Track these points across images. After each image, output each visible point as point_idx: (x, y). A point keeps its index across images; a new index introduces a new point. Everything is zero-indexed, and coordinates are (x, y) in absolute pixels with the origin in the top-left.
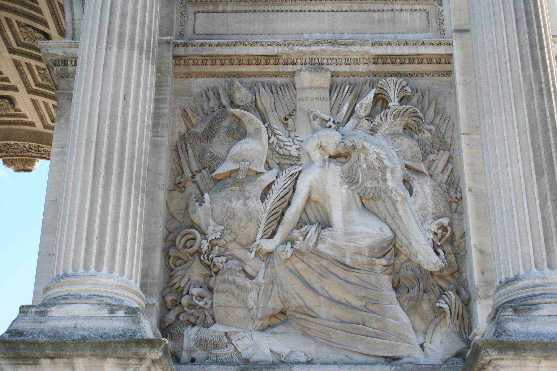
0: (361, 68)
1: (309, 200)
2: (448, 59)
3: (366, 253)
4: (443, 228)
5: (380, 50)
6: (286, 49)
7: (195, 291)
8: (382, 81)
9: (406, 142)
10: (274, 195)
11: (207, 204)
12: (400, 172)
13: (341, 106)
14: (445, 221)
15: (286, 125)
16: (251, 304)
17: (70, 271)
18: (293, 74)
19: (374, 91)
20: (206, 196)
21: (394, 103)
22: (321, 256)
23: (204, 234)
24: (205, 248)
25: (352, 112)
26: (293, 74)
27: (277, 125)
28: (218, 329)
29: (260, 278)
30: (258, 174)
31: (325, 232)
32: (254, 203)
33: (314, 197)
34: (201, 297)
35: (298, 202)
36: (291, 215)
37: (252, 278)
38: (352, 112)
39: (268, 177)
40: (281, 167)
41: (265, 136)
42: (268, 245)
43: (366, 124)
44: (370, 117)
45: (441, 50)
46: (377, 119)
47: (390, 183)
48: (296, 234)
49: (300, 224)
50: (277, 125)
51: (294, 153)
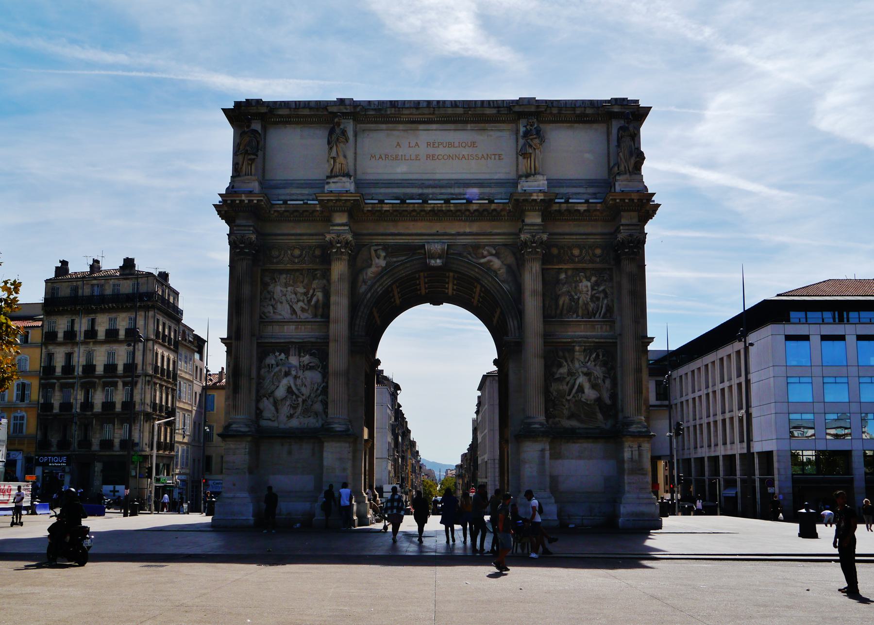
0: (592, 344)
1: (579, 386)
2: (616, 342)
3: (593, 401)
4: (612, 393)
5: (597, 340)
6: (572, 340)
7: (551, 410)
8: (598, 351)
9: (604, 369)
10: (569, 385)
11: (553, 387)
12: (602, 377)
13: (587, 357)
14: (612, 391)
15: (572, 363)
16: (564, 413)
17: (532, 416)
18: (574, 346)
19: (595, 353)
20: (553, 384)
21: (601, 357)
22: (582, 402)
23: (552, 394)
24: (553, 398)
25: (589, 359)
26: (574, 346)
27: (570, 363)
28: (557, 419)
29: (567, 406)
30: (566, 378)
31: (583, 395)
32: (565, 387)
33: (580, 385)
34: (552, 411)
35: (576, 387)
36: (574, 391)
37: (565, 406)
38: (589, 359)
39: (568, 379)
40: (572, 376)
41: (566, 366)
42: (569, 398)
43: (593, 363)
44: (594, 361)
45: (614, 341)
46: (596, 363)
47: (599, 382)
48: (576, 395)
49: (576, 393)
50: (570, 363)
51: (575, 372)
